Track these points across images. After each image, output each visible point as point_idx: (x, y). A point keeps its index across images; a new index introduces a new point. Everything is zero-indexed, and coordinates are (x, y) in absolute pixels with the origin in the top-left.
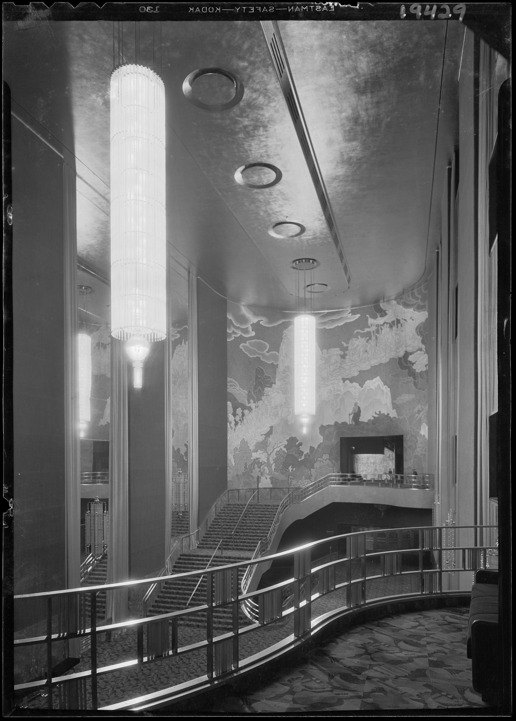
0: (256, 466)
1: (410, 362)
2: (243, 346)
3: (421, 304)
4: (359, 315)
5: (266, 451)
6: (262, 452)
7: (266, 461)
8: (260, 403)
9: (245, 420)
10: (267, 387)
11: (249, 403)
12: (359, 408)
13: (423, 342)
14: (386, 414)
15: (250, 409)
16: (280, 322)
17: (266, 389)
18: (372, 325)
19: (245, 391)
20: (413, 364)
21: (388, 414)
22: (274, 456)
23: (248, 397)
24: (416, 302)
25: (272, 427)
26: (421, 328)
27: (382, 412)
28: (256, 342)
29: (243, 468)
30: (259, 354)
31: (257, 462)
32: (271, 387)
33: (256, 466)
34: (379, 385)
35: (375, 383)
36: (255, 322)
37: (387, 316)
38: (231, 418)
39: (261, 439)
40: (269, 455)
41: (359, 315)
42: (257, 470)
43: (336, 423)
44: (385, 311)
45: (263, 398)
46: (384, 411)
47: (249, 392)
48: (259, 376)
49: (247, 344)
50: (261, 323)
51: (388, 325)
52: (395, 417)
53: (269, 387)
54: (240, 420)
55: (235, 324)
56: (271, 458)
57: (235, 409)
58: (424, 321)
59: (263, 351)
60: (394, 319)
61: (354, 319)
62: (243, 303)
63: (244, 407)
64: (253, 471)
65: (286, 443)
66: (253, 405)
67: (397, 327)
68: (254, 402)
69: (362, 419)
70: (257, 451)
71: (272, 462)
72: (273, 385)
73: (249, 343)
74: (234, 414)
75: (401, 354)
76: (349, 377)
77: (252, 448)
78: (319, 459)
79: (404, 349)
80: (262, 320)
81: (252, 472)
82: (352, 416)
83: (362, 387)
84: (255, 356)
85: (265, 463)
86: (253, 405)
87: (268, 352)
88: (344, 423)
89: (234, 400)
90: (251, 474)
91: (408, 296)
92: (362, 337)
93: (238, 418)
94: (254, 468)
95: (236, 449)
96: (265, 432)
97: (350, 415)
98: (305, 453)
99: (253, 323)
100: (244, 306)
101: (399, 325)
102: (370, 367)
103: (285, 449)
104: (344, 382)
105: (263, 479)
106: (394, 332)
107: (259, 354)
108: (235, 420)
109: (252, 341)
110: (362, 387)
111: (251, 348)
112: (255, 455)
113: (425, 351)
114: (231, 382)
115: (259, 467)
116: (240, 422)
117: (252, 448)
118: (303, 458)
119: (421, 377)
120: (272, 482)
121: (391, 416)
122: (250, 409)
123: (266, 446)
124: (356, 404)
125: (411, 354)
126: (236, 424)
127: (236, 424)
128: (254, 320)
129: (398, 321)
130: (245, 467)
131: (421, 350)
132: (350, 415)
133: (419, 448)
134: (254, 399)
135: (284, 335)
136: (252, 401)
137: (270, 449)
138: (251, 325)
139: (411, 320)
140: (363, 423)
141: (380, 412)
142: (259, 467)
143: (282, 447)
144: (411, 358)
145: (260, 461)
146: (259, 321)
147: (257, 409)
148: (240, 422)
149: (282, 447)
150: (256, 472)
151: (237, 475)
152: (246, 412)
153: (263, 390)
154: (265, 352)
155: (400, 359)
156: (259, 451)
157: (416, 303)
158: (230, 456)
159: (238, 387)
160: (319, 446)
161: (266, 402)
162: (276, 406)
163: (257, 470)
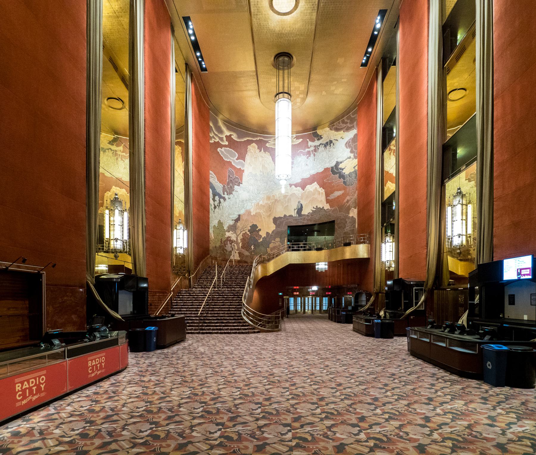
0: (228, 242)
1: (340, 169)
3: (349, 126)
4: (302, 140)
5: (235, 233)
7: (235, 240)
8: (231, 196)
9: (221, 206)
11: (224, 194)
12: (301, 205)
13: (352, 152)
18: (311, 146)
20: (343, 169)
21: (323, 207)
22: (241, 237)
24: (345, 125)
25: (239, 215)
26: (350, 142)
27: (318, 207)
29: (219, 242)
31: (228, 239)
32: (239, 185)
33: (228, 242)
36: (228, 135)
37: (322, 139)
38: (211, 202)
39: (232, 223)
40: (238, 236)
41: (302, 140)
42: (229, 245)
43: (285, 216)
44: (321, 136)
45: (234, 193)
47: (224, 186)
51: (323, 145)
52: (328, 209)
53: (238, 185)
54: (218, 205)
56: (239, 238)
58: (352, 137)
59: (234, 158)
60: (328, 140)
61: (298, 142)
62: (221, 116)
63: (220, 197)
64: (227, 246)
65: (250, 228)
67: (330, 146)
68: (227, 194)
69: (303, 213)
70: (229, 232)
71: (239, 241)
72: (241, 184)
74: (214, 200)
75: (333, 164)
76: (295, 183)
77: (225, 228)
78: (273, 241)
79: (336, 160)
81: (226, 247)
82: (296, 211)
83: (304, 190)
86: (226, 196)
87: (237, 159)
88: (291, 216)
89: (214, 189)
90: (225, 248)
91: (339, 123)
92: (304, 155)
93: (216, 203)
94: (227, 244)
97: (295, 210)
98: (263, 237)
100: (221, 119)
101: (332, 144)
102: (309, 176)
103: (248, 233)
104: (290, 187)
106: (327, 149)
107: (232, 160)
108: (214, 204)
110: (304, 190)
112: (228, 234)
113: (353, 157)
115: (231, 244)
116: (217, 207)
117: (225, 228)
119: (349, 176)
121: (325, 208)
123: (236, 229)
124: (299, 202)
125: (341, 163)
126: (215, 207)
127: (215, 207)
129: (331, 142)
130: (221, 242)
131: (350, 158)
132: (295, 210)
133: (348, 226)
134: (227, 192)
136: (226, 193)
137: (238, 232)
139: (342, 139)
140: (304, 215)
141: (317, 206)
142: (231, 244)
143: (247, 231)
144: (341, 166)
148: (217, 207)
149: (247, 231)
150: (228, 247)
151: (216, 247)
152: (222, 200)
153: (234, 187)
154: (235, 159)
155: (332, 168)
156: (231, 232)
157: (345, 127)
158: (211, 231)
159: (216, 180)
160: (273, 232)
161: (236, 196)
163: (229, 245)
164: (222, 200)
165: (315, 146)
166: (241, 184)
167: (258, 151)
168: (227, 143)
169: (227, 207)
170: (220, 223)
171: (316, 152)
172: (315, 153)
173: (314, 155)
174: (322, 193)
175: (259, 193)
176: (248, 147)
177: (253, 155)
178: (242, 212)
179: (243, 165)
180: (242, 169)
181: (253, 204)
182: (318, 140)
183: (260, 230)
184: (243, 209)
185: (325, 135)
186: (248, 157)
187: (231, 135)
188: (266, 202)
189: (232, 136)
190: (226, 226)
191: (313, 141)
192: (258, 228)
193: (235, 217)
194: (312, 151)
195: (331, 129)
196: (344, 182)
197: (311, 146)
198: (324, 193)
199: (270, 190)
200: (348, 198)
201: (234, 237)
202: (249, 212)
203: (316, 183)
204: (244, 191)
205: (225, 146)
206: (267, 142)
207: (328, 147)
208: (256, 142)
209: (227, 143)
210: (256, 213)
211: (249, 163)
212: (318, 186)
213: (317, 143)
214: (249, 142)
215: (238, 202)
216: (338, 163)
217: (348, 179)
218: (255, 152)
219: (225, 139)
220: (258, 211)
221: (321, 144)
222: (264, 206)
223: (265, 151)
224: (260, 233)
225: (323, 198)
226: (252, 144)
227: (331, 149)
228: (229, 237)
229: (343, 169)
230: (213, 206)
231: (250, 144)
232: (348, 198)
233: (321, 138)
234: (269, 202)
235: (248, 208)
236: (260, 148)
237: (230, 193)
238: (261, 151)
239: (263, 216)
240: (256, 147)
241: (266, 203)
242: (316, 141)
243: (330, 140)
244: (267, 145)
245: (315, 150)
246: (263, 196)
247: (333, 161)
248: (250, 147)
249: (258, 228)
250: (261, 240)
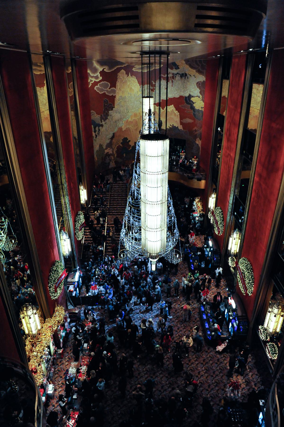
0: (107, 157)
2: (96, 88)
5: (111, 148)
6: (110, 149)
9: (100, 133)
11: (101, 122)
14: (176, 127)
15: (102, 126)
16: (116, 68)
17: (110, 112)
19: (99, 115)
22: (116, 149)
23: (101, 119)
25: (114, 134)
28: (103, 83)
30: (105, 91)
32: (112, 110)
33: (107, 157)
34: (173, 109)
35: (171, 108)
36: (101, 70)
40: (113, 150)
45: (108, 117)
46: (176, 125)
47: (101, 116)
48: (106, 105)
49: (98, 86)
50: (105, 70)
55: (91, 75)
59: (107, 88)
66: (103, 123)
70: (107, 149)
71: (115, 153)
72: (114, 109)
73: (100, 85)
80: (105, 68)
84: (103, 93)
85: (111, 154)
86: (103, 123)
87: (109, 89)
94: (106, 158)
96: (110, 137)
98: (132, 146)
99: (101, 71)
105: (111, 163)
109: (101, 83)
111: (100, 88)
112: (106, 151)
114: (92, 113)
116: (98, 135)
118: (131, 148)
120: (116, 163)
128: (100, 69)
135: (118, 76)
136: (103, 120)
137: (113, 146)
138: (100, 73)
142: (109, 157)
146: (104, 69)
147: (106, 124)
150: (107, 161)
161: (110, 120)
163: (108, 158)
165: (173, 74)
169: (105, 131)
171: (174, 79)
172: (173, 80)
173: (172, 82)
174: (177, 115)
175: (128, 112)
177: (122, 81)
178: (116, 130)
179: (114, 92)
180: (114, 95)
181: (124, 122)
182: (176, 69)
183: (130, 141)
185: (181, 66)
186: (118, 84)
188: (133, 118)
190: (105, 146)
191: (172, 69)
192: (128, 140)
193: (111, 135)
194: (171, 77)
195: (186, 63)
196: (194, 114)
197: (170, 73)
198: (179, 116)
199: (137, 109)
200: (195, 128)
202: (121, 129)
203: (173, 105)
207: (183, 78)
210: (126, 129)
211: (119, 88)
212: (174, 109)
213: (175, 71)
214: (119, 70)
215: (112, 123)
216: (190, 96)
217: (197, 113)
218: (124, 78)
220: (128, 126)
221: (178, 73)
222: (132, 122)
223: (131, 75)
224: (130, 143)
225: (178, 119)
226: (121, 72)
227: (186, 81)
228: (108, 153)
229: (194, 103)
230: (95, 136)
232: (195, 128)
233: (179, 68)
234: (136, 119)
235: (120, 126)
236: (127, 74)
238: (128, 75)
239: (131, 130)
240: (125, 72)
241: (134, 120)
242: (174, 70)
243: (185, 73)
244: (134, 69)
245: (173, 78)
246: (131, 114)
247: (187, 92)
248: (119, 74)
249: (128, 140)
250: (131, 148)
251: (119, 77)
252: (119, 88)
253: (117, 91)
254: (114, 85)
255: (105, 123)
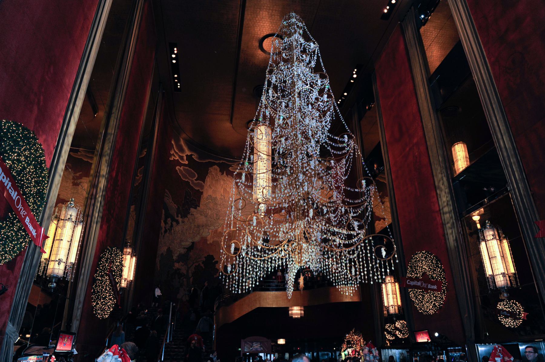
6: (183, 264)
8: (186, 220)
9: (172, 231)
10: (192, 207)
11: (178, 216)
19: (175, 205)
25: (193, 243)
32: (196, 208)
38: (163, 224)
39: (183, 251)
45: (189, 216)
54: (169, 229)
57: (166, 217)
59: (192, 178)
63: (173, 219)
68: (181, 217)
72: (198, 207)
74: (166, 223)
86: (180, 219)
87: (196, 180)
93: (168, 226)
95: (162, 254)
108: (165, 227)
112: (177, 265)
116: (168, 231)
122: (178, 222)
126: (166, 231)
127: (166, 231)
136: (180, 215)
145: (181, 272)
152: (174, 223)
154: (194, 179)
156: (181, 263)
158: (158, 261)
161: (191, 220)
162: (199, 226)
164: (174, 223)
166: (198, 207)
167: (220, 173)
168: (187, 162)
169: (180, 232)
170: (170, 251)
176: (210, 168)
178: (197, 239)
184: (199, 236)
186: (208, 180)
187: (192, 155)
189: (193, 156)
190: (176, 255)
193: (188, 243)
201: (184, 271)
204: (201, 215)
205: (185, 165)
206: (230, 166)
208: (219, 165)
209: (187, 162)
211: (209, 185)
215: (193, 226)
219: (185, 158)
228: (178, 269)
230: (163, 230)
231: (211, 166)
237: (184, 216)
238: (223, 174)
240: (218, 169)
248: (211, 169)
251: (211, 172)
252: (208, 184)
253: (206, 188)
254: (202, 177)
255: (183, 222)
